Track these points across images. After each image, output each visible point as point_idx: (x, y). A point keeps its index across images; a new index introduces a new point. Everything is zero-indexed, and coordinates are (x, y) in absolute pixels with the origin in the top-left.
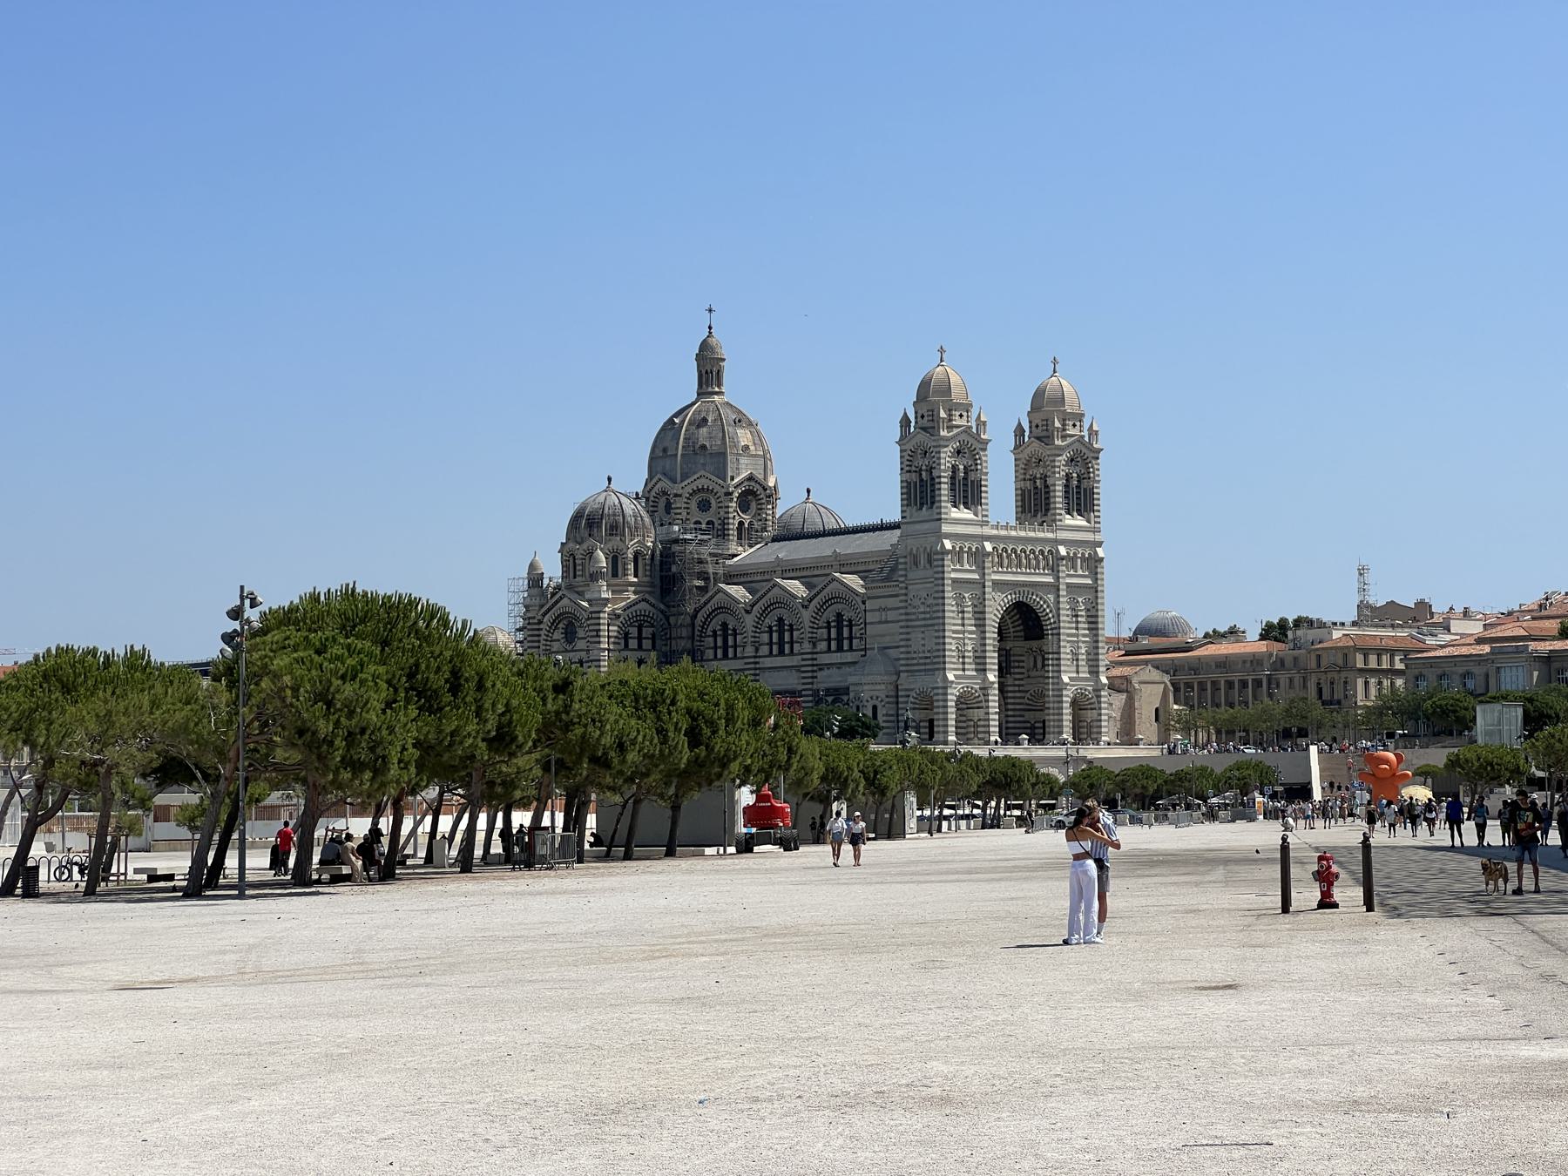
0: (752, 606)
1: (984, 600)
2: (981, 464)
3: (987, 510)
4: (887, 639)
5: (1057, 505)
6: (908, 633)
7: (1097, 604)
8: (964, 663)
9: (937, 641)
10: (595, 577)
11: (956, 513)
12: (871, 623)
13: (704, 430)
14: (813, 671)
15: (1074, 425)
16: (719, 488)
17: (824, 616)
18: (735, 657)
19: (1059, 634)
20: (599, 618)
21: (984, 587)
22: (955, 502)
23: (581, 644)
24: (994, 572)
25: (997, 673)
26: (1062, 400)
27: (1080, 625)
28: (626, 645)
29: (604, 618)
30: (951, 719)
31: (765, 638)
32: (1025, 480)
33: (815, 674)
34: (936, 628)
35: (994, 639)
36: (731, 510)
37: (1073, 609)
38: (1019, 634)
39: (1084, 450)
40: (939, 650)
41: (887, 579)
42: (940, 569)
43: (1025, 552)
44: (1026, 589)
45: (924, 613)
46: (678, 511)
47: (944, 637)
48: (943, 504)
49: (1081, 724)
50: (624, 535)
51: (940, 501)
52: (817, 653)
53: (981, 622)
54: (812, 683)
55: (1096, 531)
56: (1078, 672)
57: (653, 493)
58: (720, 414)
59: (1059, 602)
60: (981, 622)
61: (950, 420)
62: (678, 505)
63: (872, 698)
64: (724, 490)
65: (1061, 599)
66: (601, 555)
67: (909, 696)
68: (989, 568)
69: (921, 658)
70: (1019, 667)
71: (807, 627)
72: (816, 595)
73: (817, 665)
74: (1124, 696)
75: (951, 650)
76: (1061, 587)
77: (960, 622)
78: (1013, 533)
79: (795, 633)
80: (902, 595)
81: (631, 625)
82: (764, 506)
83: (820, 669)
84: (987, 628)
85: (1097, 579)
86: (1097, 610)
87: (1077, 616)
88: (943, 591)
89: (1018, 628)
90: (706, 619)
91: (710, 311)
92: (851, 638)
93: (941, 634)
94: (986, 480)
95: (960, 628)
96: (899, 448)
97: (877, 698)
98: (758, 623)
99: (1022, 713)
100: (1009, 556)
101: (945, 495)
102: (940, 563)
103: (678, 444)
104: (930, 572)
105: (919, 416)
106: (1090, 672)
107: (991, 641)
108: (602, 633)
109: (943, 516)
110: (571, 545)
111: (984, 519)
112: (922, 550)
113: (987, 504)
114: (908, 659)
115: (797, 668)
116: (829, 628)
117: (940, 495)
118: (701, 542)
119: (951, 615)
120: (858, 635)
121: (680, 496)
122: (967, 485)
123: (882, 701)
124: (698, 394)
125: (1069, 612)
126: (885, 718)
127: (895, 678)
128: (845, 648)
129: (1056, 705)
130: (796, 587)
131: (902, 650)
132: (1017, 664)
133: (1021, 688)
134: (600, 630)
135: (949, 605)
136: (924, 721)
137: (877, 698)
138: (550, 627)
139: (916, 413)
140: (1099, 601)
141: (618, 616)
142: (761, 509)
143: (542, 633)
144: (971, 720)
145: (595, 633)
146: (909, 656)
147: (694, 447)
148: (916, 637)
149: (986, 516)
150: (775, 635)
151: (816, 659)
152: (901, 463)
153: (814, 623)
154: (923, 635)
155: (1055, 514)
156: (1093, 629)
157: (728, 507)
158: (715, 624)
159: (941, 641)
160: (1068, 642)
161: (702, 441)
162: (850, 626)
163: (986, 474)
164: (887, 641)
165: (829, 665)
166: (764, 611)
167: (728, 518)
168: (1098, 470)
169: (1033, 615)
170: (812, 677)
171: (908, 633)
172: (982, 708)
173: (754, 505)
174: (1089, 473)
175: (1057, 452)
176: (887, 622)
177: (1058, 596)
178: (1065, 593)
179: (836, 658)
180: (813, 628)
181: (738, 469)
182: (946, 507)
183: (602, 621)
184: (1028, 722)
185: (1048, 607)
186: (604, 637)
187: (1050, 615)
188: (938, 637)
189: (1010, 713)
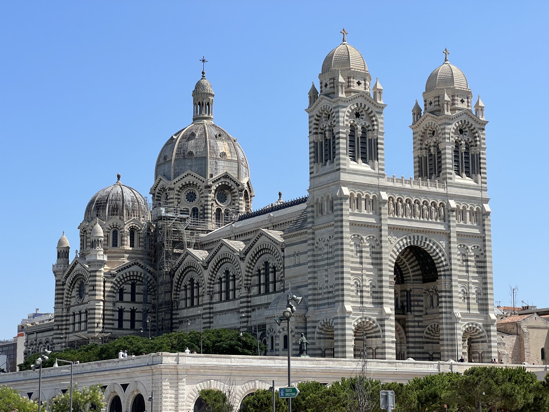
0: (208, 263)
1: (381, 242)
2: (377, 125)
3: (383, 165)
4: (299, 279)
5: (448, 166)
6: (315, 272)
7: (485, 251)
8: (362, 297)
9: (337, 276)
10: (93, 244)
11: (353, 165)
12: (289, 267)
13: (192, 142)
14: (248, 312)
15: (462, 101)
16: (201, 182)
17: (256, 266)
18: (198, 305)
19: (450, 275)
20: (96, 276)
21: (381, 230)
22: (354, 157)
23: (86, 298)
24: (390, 218)
25: (393, 307)
26: (451, 80)
27: (470, 269)
28: (121, 299)
29: (100, 276)
30: (350, 346)
31: (217, 287)
32: (421, 149)
33: (250, 314)
34: (336, 265)
35: (390, 276)
36: (209, 199)
37: (464, 255)
38: (418, 277)
39: (471, 122)
40: (338, 284)
41: (301, 228)
42: (339, 212)
43: (418, 203)
44: (420, 235)
45: (327, 253)
47: (343, 273)
48: (341, 156)
49: (474, 355)
50: (123, 215)
51: (339, 154)
52: (251, 297)
53: (378, 261)
54: (247, 322)
55: (482, 190)
56: (469, 309)
57: (157, 191)
58: (205, 131)
59: (450, 248)
60: (378, 261)
61: (349, 86)
62: (171, 196)
64: (204, 184)
65: (452, 245)
66: (98, 227)
67: (315, 327)
68: (385, 214)
69: (325, 293)
70: (418, 306)
71: (244, 275)
72: (250, 249)
73: (251, 307)
74: (514, 338)
75: (349, 284)
76: (452, 234)
77: (358, 260)
78: (408, 186)
79: (237, 282)
80: (309, 239)
81: (125, 283)
82: (237, 198)
83: (254, 310)
84: (384, 267)
85: (484, 230)
86: (485, 256)
87: (467, 261)
88: (342, 232)
89: (417, 273)
90: (180, 277)
91: (204, 61)
92: (274, 282)
93: (340, 270)
94: (383, 139)
95: (358, 265)
96: (307, 115)
98: (212, 276)
99: (421, 345)
100: (404, 206)
101: (343, 149)
102: (339, 207)
103: (173, 152)
104: (332, 217)
105: (323, 85)
106: (480, 310)
107: (388, 278)
108: (97, 288)
109: (342, 167)
110: (84, 223)
111: (381, 172)
112: (325, 198)
113: (383, 160)
114: (314, 295)
115: (237, 310)
116: (259, 275)
117: (339, 148)
118: (183, 220)
119: (349, 253)
120: (280, 278)
121: (173, 189)
122: (365, 143)
124: (194, 120)
125: (459, 257)
127: (303, 312)
128: (271, 290)
129: (449, 337)
130: (239, 246)
131: (310, 287)
132: (416, 303)
133: (420, 324)
134: (95, 285)
135: (348, 244)
136: (328, 349)
138: (70, 287)
139: (321, 83)
140: (487, 248)
141: (114, 276)
142: (234, 200)
143: (65, 292)
144: (370, 348)
145: (92, 288)
146: (316, 292)
147: (184, 153)
148: (321, 275)
149: (383, 170)
150: (223, 285)
151: (250, 302)
152: (310, 127)
153: (248, 272)
154: (326, 273)
155: (446, 173)
156: (481, 273)
157: (207, 197)
158: (186, 281)
159: (340, 276)
160: (460, 282)
161: (190, 149)
162: (274, 272)
163: (382, 134)
164: (299, 281)
165: (259, 306)
166: (216, 266)
167: (207, 205)
168: (484, 139)
169: (429, 261)
170: (248, 317)
171: (315, 272)
172: (380, 337)
173: (229, 197)
174: (476, 141)
175: (447, 121)
176: (299, 265)
177: (450, 242)
178: (455, 240)
179: (264, 299)
180: (248, 276)
181: (216, 169)
182: (345, 159)
183: (97, 278)
184: (428, 353)
185: (440, 251)
186: (100, 290)
187: (443, 259)
188: (337, 273)
189: (411, 345)
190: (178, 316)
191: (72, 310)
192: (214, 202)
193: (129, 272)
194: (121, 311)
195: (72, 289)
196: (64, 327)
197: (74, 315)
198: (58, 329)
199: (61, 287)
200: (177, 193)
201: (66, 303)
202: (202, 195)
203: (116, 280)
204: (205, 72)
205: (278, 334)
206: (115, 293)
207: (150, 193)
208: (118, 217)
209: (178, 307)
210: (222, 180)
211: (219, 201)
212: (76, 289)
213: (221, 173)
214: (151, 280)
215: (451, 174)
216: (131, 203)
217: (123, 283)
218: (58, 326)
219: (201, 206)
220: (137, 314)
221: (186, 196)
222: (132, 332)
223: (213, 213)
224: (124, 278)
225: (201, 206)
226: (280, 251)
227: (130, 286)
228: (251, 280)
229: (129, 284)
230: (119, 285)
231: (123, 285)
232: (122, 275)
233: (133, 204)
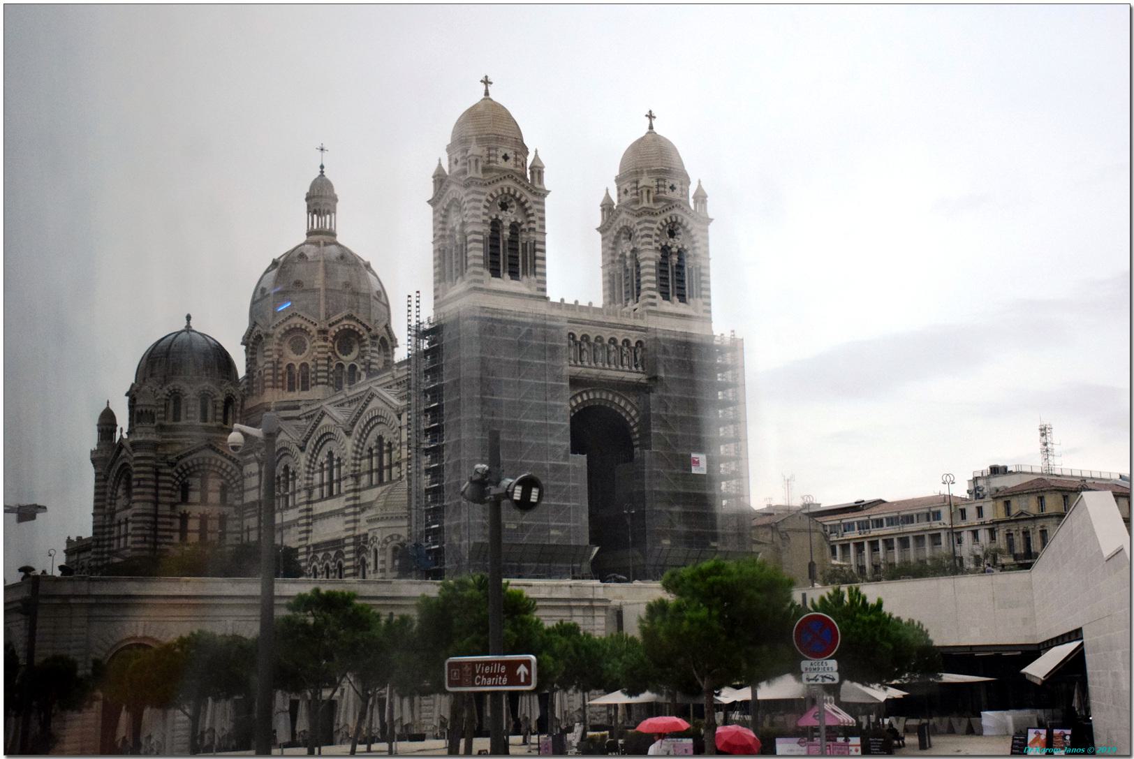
0: (306, 441)
11: (497, 284)
14: (355, 513)
16: (311, 327)
17: (366, 444)
32: (613, 262)
46: (270, 353)
54: (354, 529)
62: (270, 347)
73: (360, 505)
79: (343, 468)
83: (363, 510)
98: (311, 461)
120: (396, 460)
124: (309, 234)
150: (326, 473)
191: (118, 516)
192: (330, 354)
195: (118, 486)
197: (119, 524)
200: (277, 341)
201: (108, 507)
202: (314, 344)
203: (177, 471)
204: (324, 164)
206: (176, 491)
207: (242, 344)
210: (345, 322)
211: (340, 352)
212: (122, 486)
213: (345, 313)
214: (232, 470)
215: (654, 297)
217: (187, 475)
219: (313, 360)
221: (292, 346)
223: (331, 370)
225: (313, 360)
226: (396, 419)
228: (360, 465)
230: (180, 479)
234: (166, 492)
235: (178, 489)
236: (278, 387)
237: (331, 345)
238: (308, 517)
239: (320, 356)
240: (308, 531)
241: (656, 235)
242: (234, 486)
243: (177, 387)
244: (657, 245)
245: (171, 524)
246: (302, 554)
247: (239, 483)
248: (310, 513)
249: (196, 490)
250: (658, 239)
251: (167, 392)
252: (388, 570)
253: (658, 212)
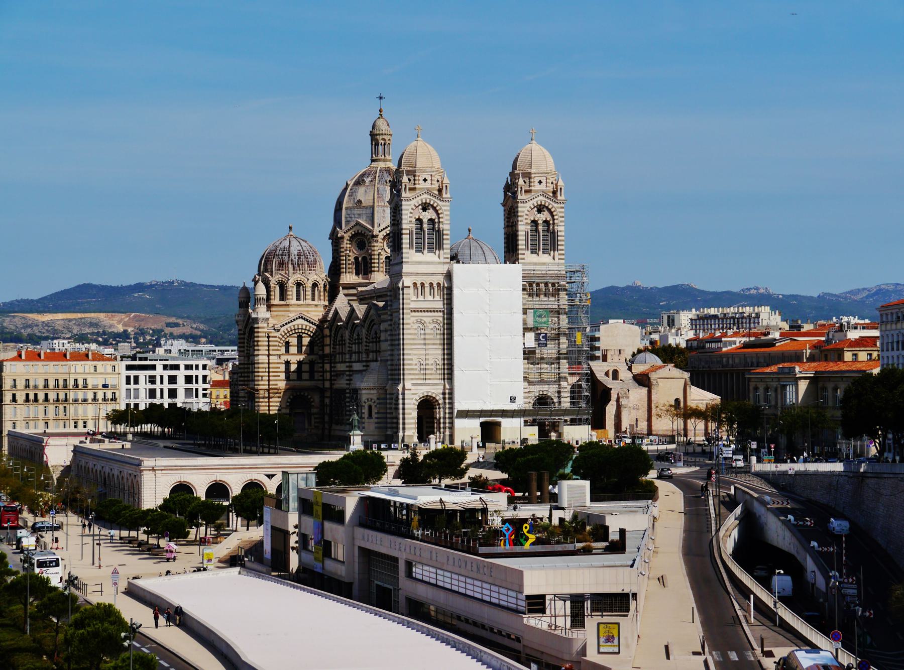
11: (418, 257)
28: (287, 351)
62: (342, 246)
63: (368, 399)
91: (381, 98)
97: (371, 399)
98: (350, 336)
123: (374, 402)
126: (376, 416)
137: (371, 399)
158: (339, 338)
182: (408, 253)
190: (335, 369)
193: (294, 326)
194: (287, 363)
196: (246, 375)
198: (241, 376)
199: (242, 336)
203: (281, 334)
205: (364, 404)
207: (329, 239)
208: (283, 273)
209: (335, 359)
215: (524, 254)
216: (297, 257)
218: (241, 373)
220: (303, 365)
222: (299, 382)
223: (381, 261)
224: (289, 332)
227: (296, 339)
228: (369, 346)
229: (295, 337)
230: (283, 339)
231: (288, 339)
232: (287, 329)
233: (299, 258)
234: (276, 348)
235: (282, 345)
236: (349, 272)
237: (382, 245)
238: (349, 371)
239: (373, 253)
240: (350, 380)
241: (527, 215)
242: (318, 342)
243: (280, 279)
244: (527, 221)
245: (279, 368)
246: (348, 393)
247: (321, 340)
248: (351, 369)
249: (293, 346)
250: (527, 217)
251: (274, 282)
252: (366, 418)
253: (527, 200)
